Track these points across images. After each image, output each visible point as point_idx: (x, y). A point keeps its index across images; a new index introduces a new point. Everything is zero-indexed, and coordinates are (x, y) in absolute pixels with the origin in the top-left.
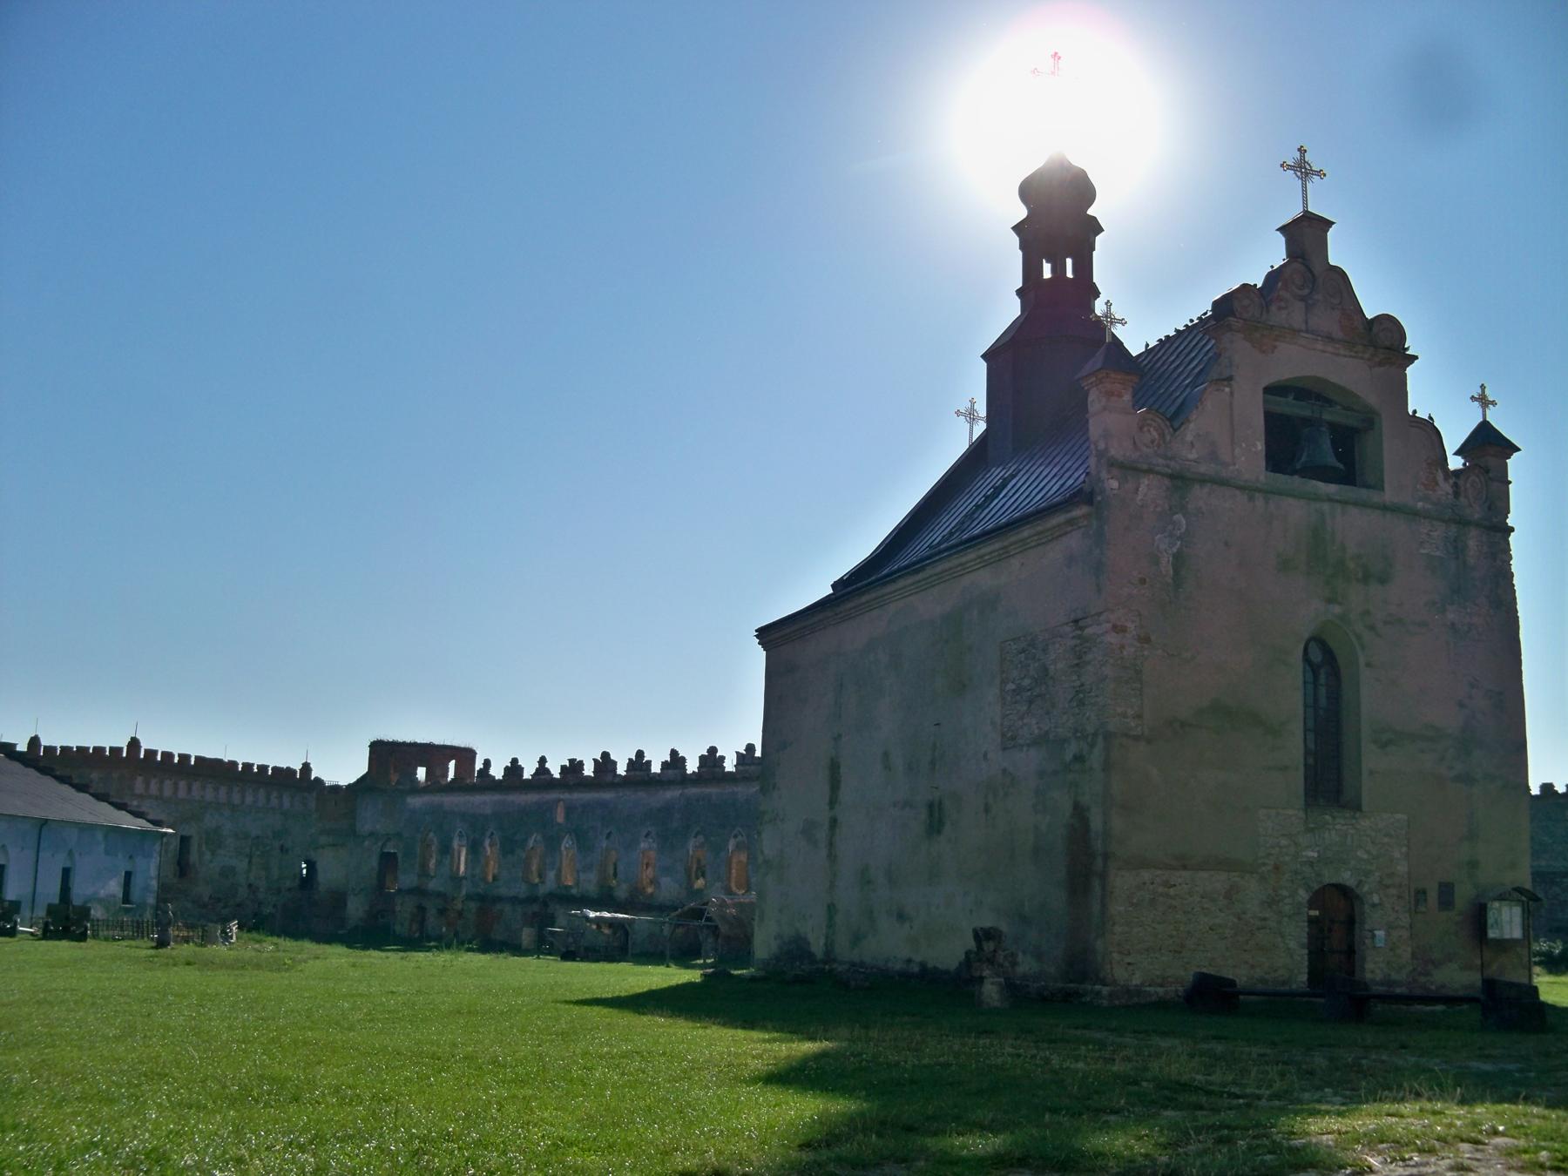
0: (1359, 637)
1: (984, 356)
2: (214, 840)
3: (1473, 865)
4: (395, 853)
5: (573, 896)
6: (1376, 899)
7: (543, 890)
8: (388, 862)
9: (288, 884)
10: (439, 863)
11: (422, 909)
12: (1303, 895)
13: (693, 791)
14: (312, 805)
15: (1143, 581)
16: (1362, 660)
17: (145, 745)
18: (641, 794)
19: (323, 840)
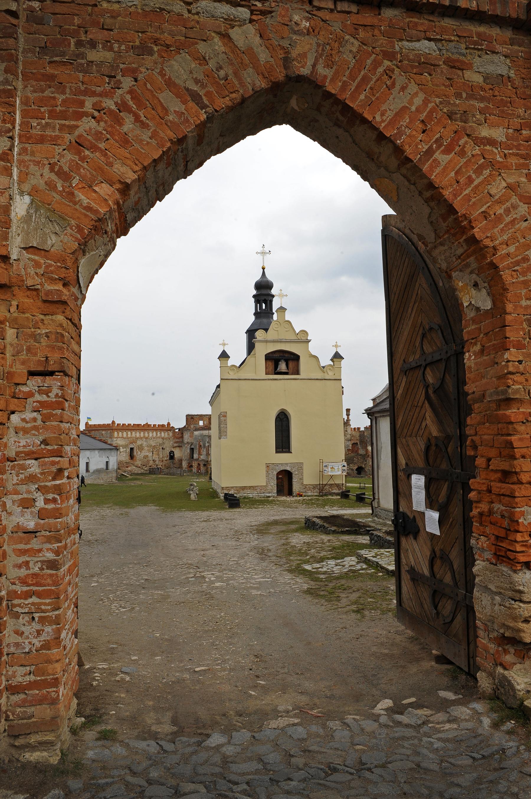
1: (246, 333)
2: (141, 448)
6: (297, 473)
8: (192, 450)
9: (165, 459)
11: (199, 464)
12: (275, 473)
14: (171, 434)
17: (117, 423)
19: (176, 445)
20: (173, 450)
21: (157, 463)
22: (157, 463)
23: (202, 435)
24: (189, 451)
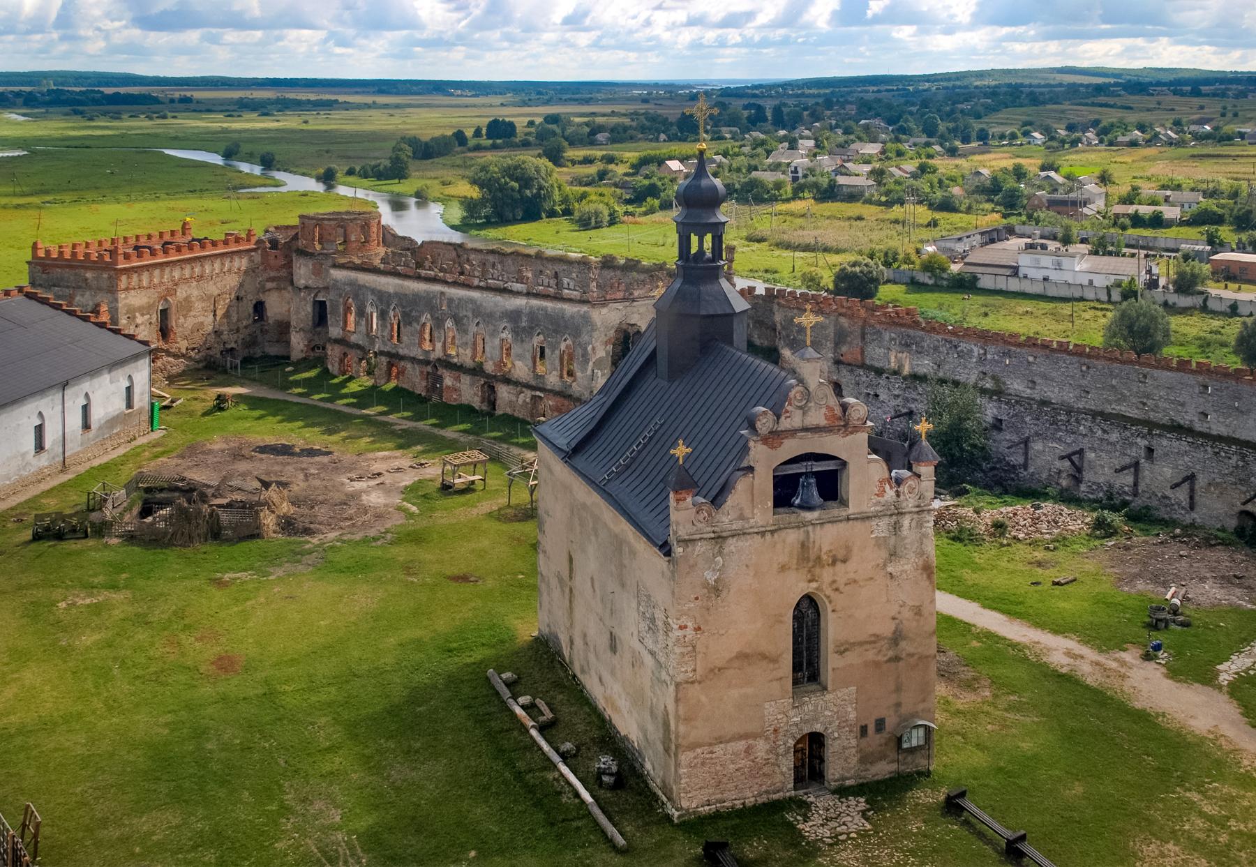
0: (828, 597)
3: (898, 705)
4: (324, 302)
5: (456, 364)
7: (433, 357)
9: (245, 323)
10: (357, 324)
13: (535, 302)
15: (697, 598)
16: (829, 610)
18: (499, 298)
19: (269, 285)
20: (262, 297)
21: (225, 337)
22: (225, 337)
23: (352, 283)
24: (309, 309)
